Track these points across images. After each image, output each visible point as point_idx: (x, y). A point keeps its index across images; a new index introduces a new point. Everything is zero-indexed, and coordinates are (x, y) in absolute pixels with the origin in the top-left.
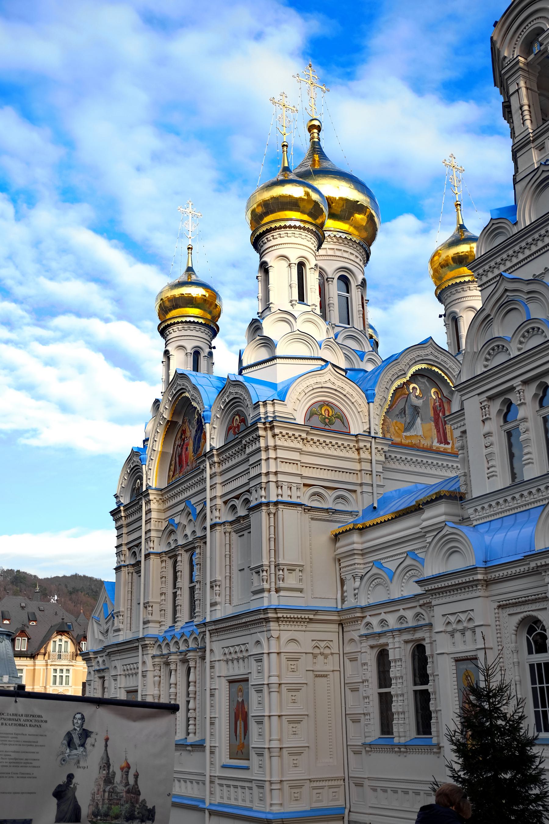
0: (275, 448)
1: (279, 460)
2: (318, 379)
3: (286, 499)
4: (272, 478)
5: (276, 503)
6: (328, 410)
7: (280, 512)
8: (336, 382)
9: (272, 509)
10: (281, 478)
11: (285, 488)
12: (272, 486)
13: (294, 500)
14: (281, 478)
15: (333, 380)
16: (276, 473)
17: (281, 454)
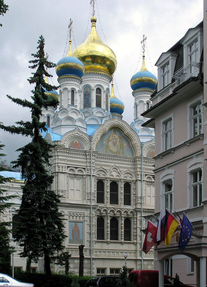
0: (58, 156)
1: (59, 159)
2: (73, 133)
3: (61, 171)
4: (57, 165)
5: (58, 172)
6: (77, 142)
7: (59, 175)
8: (80, 133)
9: (56, 174)
10: (59, 165)
11: (61, 168)
12: (57, 167)
13: (64, 171)
14: (59, 165)
15: (78, 133)
16: (58, 163)
17: (60, 157)
